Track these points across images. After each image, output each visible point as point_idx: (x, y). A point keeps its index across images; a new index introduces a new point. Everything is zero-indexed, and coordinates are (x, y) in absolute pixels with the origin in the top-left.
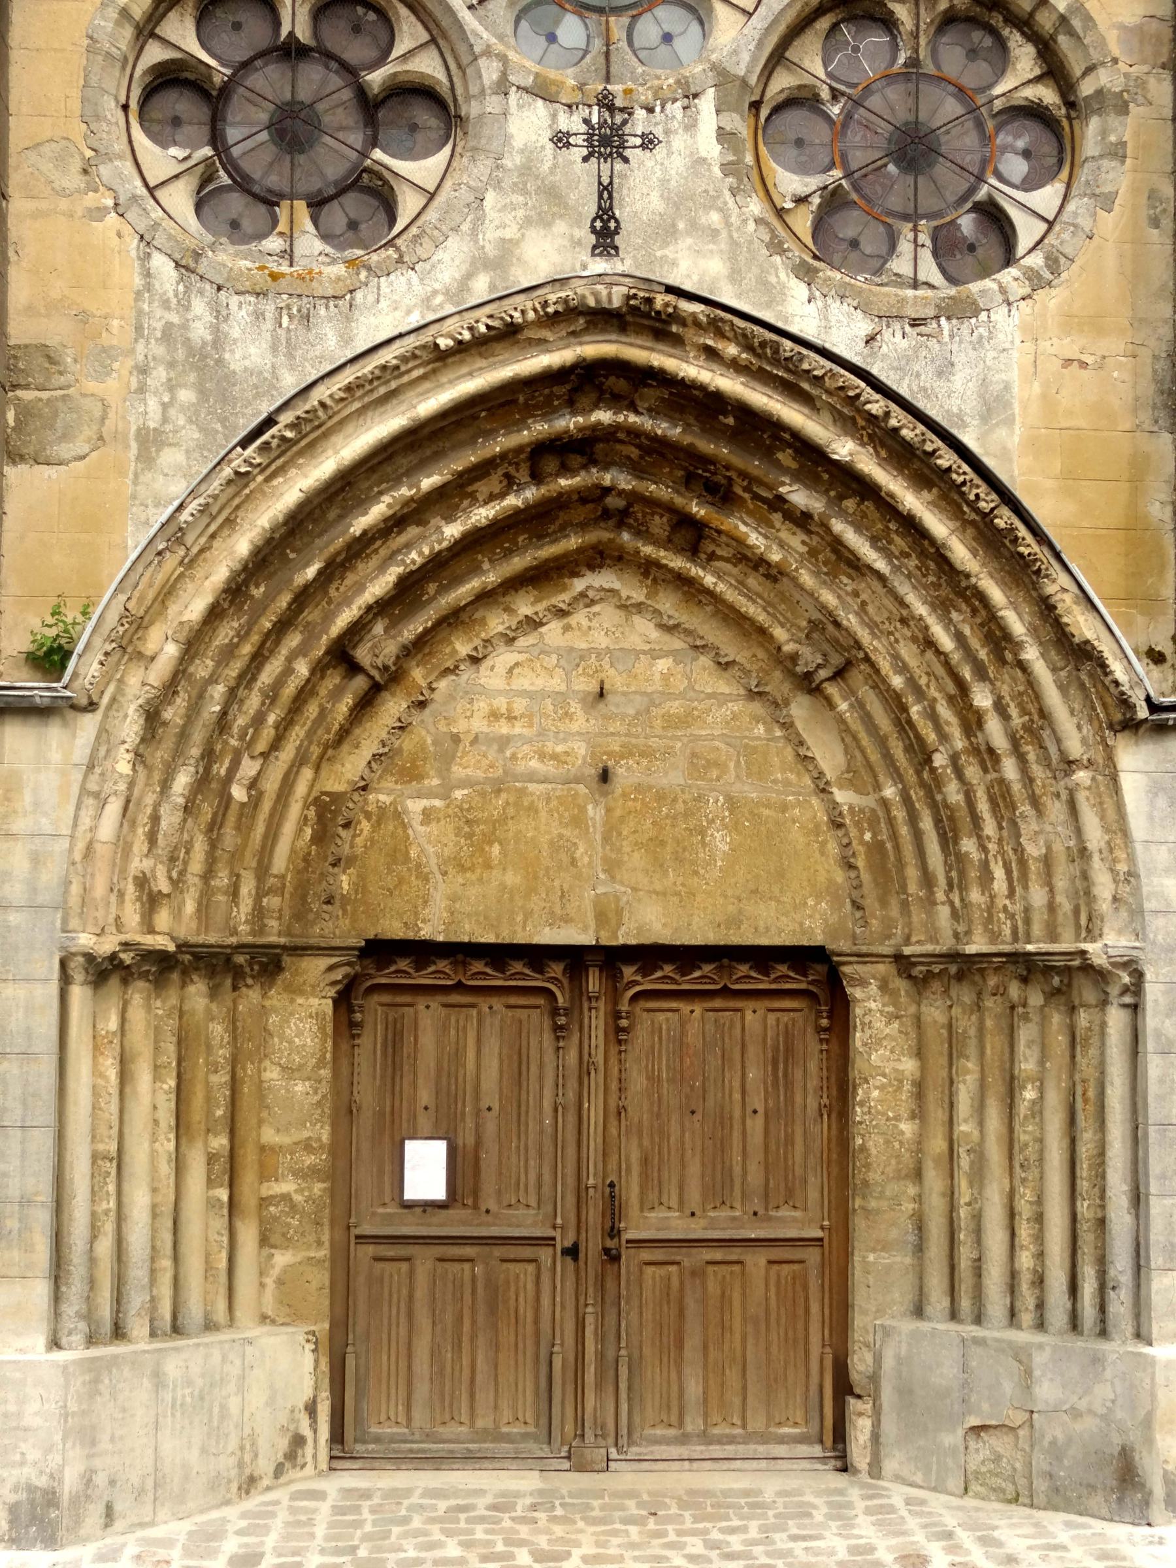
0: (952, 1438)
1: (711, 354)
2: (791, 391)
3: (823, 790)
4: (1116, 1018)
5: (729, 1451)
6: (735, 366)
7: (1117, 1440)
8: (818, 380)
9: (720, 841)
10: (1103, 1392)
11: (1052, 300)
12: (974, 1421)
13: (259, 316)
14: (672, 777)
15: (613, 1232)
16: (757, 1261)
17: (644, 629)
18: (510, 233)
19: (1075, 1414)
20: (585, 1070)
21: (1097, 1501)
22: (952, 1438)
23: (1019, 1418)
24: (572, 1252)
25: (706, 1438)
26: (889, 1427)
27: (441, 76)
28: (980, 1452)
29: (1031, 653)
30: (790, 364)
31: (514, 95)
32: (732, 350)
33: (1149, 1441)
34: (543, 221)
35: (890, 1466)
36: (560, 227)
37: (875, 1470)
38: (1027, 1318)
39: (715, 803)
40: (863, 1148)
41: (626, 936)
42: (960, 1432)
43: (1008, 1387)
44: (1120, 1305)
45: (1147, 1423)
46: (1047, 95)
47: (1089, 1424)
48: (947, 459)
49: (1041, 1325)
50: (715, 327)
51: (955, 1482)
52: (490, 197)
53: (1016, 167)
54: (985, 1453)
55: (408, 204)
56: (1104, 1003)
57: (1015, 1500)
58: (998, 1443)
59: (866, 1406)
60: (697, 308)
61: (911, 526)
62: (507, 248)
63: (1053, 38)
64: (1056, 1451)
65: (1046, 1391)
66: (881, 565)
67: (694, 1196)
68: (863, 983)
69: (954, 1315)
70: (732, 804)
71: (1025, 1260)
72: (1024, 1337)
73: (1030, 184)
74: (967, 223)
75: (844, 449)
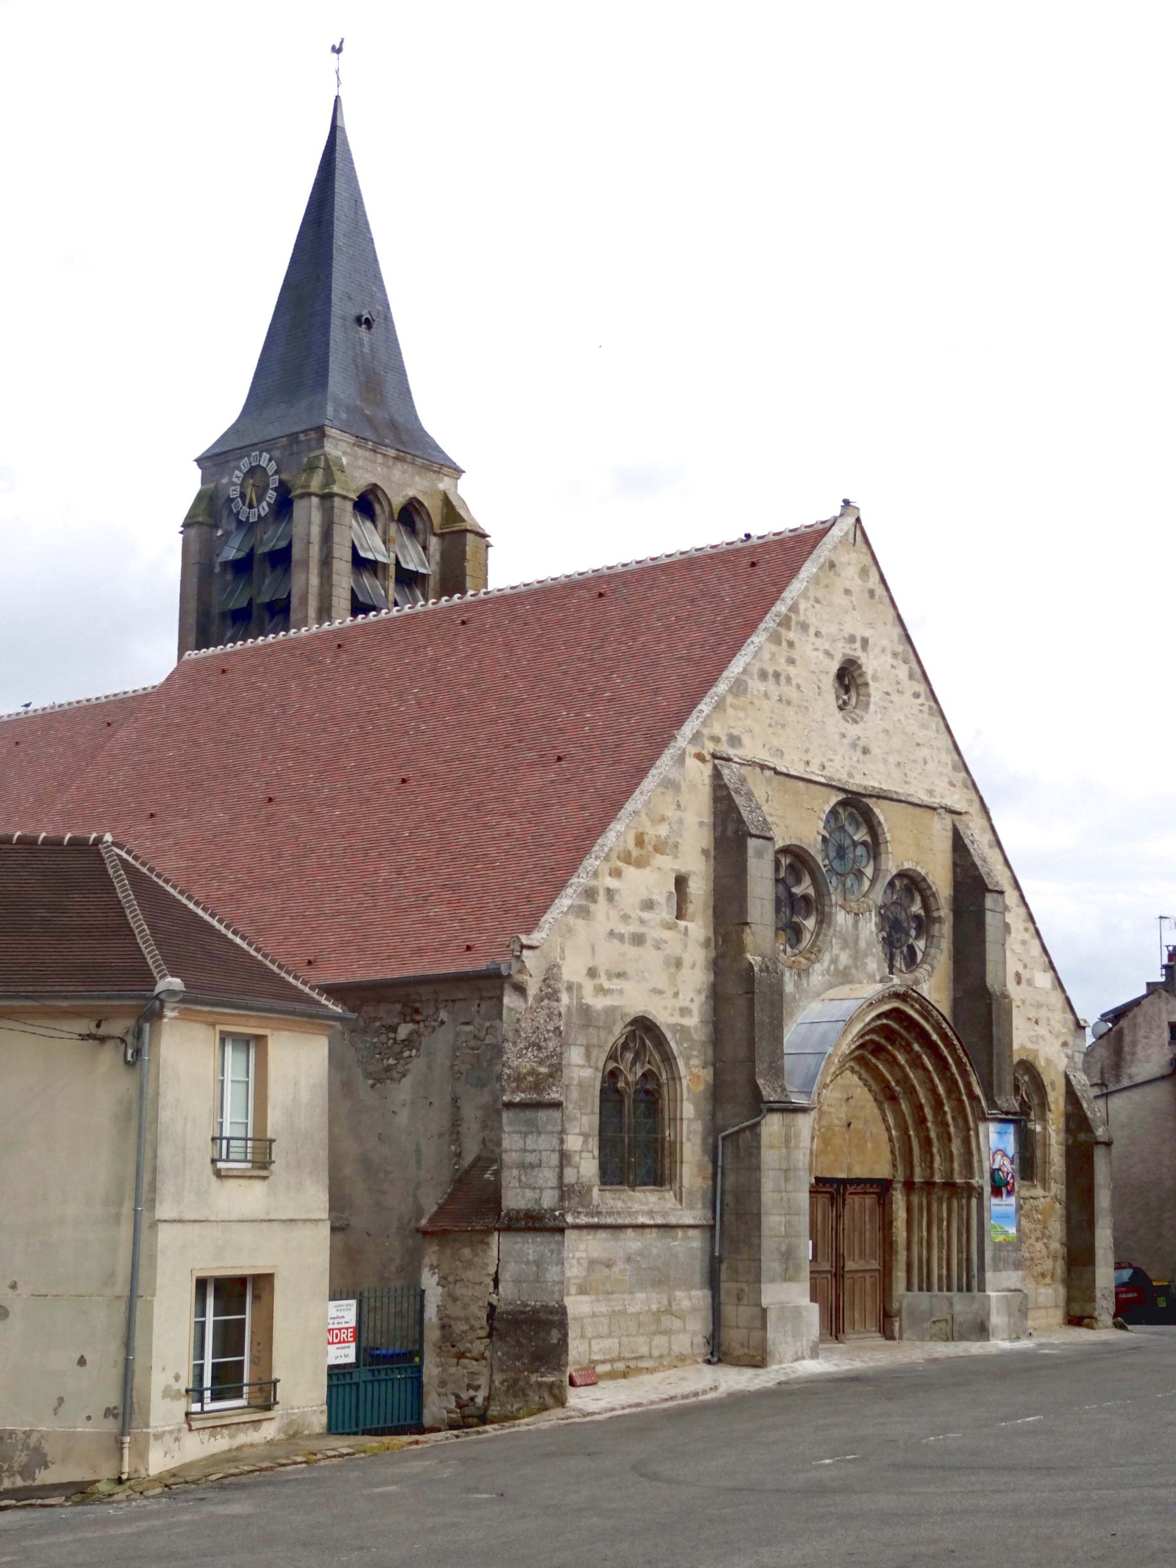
0: (928, 1324)
1: (912, 1006)
2: (927, 1021)
3: (888, 1129)
4: (974, 1202)
5: (861, 1336)
6: (916, 1011)
7: (979, 1320)
8: (932, 1016)
9: (869, 1145)
10: (975, 1306)
11: (933, 980)
12: (934, 1319)
13: (791, 975)
14: (860, 1126)
15: (843, 1267)
16: (867, 1276)
17: (855, 1078)
18: (837, 952)
19: (967, 1313)
20: (838, 1217)
21: (973, 1336)
22: (928, 1324)
23: (949, 1317)
24: (835, 1275)
25: (860, 1333)
26: (905, 1323)
27: (813, 894)
28: (936, 1327)
29: (965, 1098)
30: (929, 1012)
31: (838, 908)
32: (917, 1006)
33: (989, 1318)
34: (843, 949)
35: (905, 1336)
36: (847, 951)
37: (901, 1338)
38: (945, 1289)
39: (868, 1133)
40: (896, 1241)
41: (853, 1176)
42: (929, 1323)
43: (945, 1308)
44: (975, 1283)
45: (988, 1314)
46: (922, 912)
47: (970, 1316)
48: (956, 1042)
49: (949, 1289)
50: (916, 1001)
51: (928, 1338)
52: (834, 940)
53: (913, 933)
54: (937, 1328)
55: (807, 938)
56: (969, 1198)
57: (947, 1340)
58: (943, 1325)
59: (897, 1319)
60: (915, 995)
61: (944, 1059)
62: (837, 956)
63: (928, 897)
64: (961, 1324)
65: (957, 1308)
66: (931, 1068)
67: (856, 1256)
68: (896, 1190)
69: (921, 1289)
70: (871, 1133)
71: (945, 1272)
72: (945, 1293)
73: (917, 938)
74: (905, 949)
75: (935, 1037)
